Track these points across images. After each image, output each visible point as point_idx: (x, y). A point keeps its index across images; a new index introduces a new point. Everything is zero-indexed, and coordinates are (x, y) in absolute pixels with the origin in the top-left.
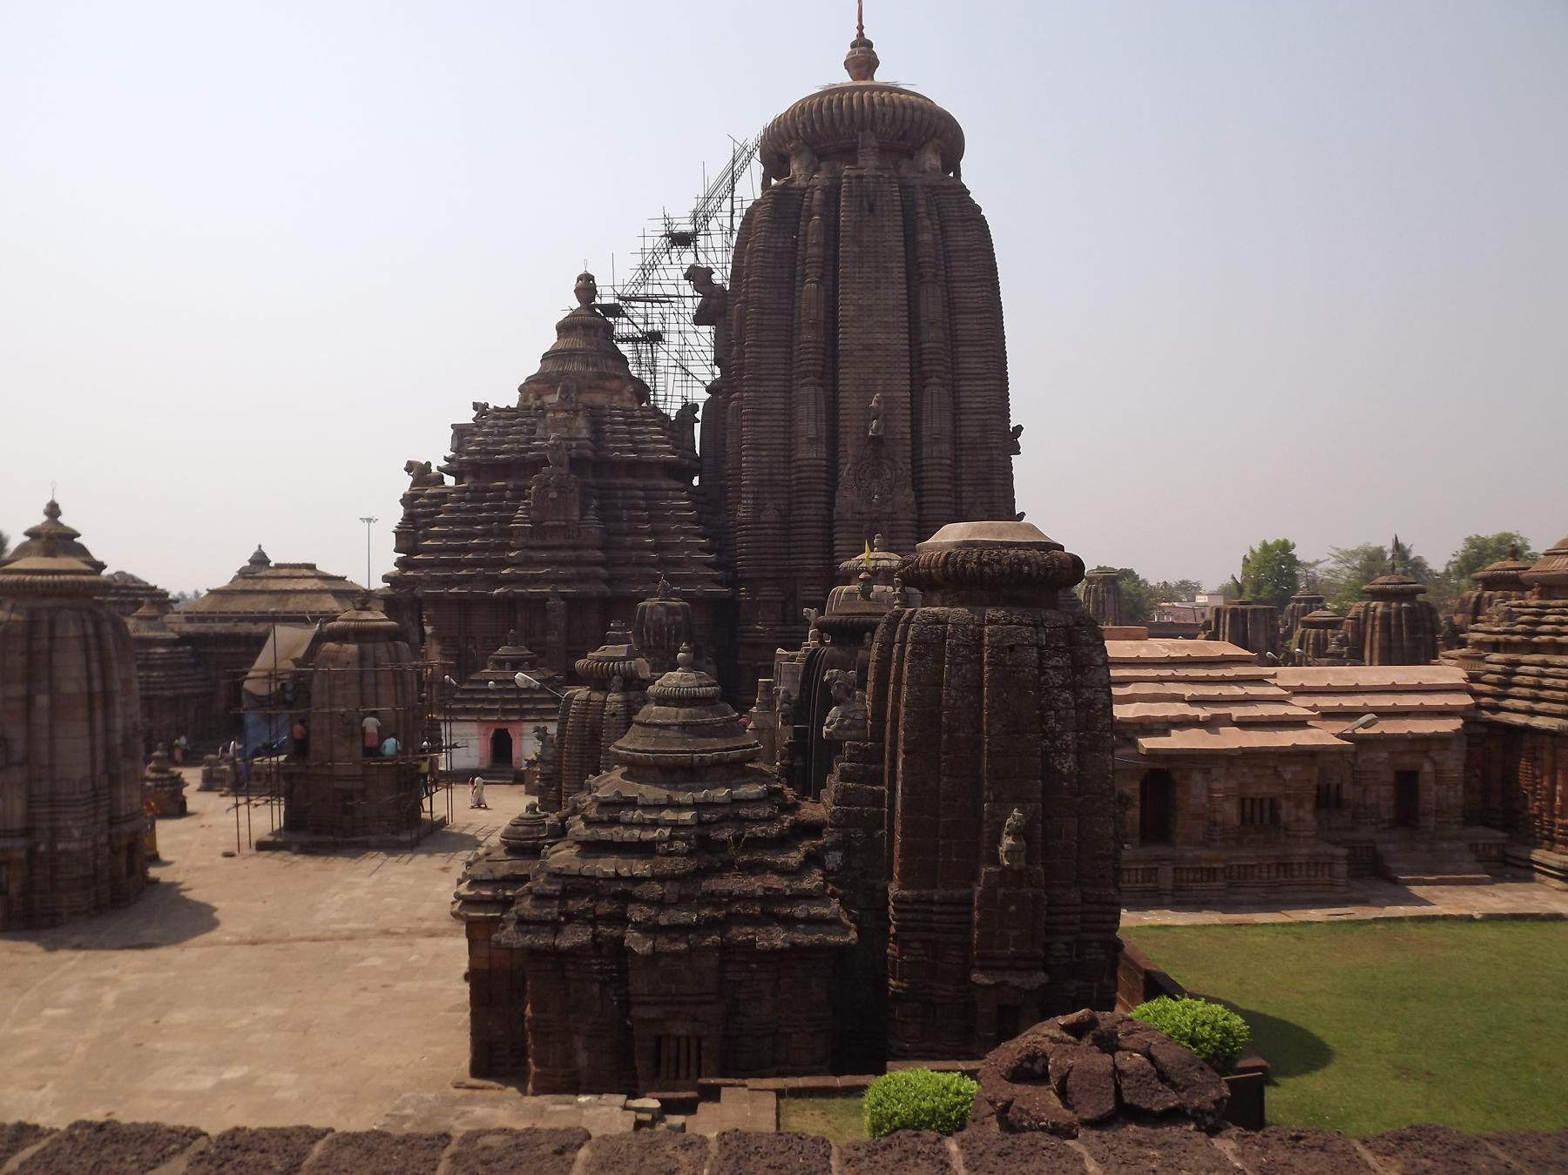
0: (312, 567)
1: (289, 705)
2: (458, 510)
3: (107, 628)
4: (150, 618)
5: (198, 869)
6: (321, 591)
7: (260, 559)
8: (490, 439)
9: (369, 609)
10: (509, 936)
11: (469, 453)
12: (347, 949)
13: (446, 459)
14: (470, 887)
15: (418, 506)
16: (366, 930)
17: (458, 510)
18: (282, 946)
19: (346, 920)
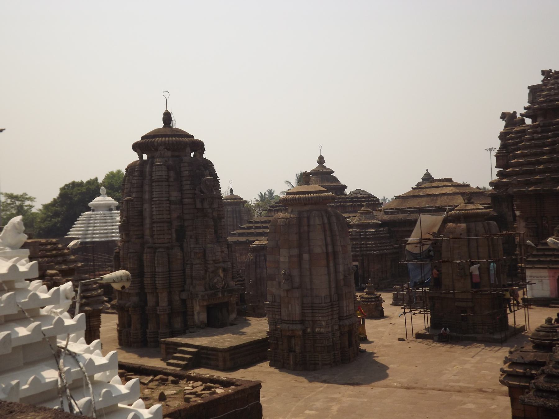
0: (450, 180)
1: (430, 258)
2: (533, 139)
3: (334, 219)
4: (366, 213)
5: (386, 346)
6: (455, 194)
7: (428, 178)
8: (552, 92)
9: (472, 203)
10: (530, 397)
11: (539, 103)
12: (456, 397)
13: (525, 108)
14: (510, 366)
15: (509, 139)
16: (470, 388)
17: (533, 139)
18: (422, 391)
19: (458, 381)
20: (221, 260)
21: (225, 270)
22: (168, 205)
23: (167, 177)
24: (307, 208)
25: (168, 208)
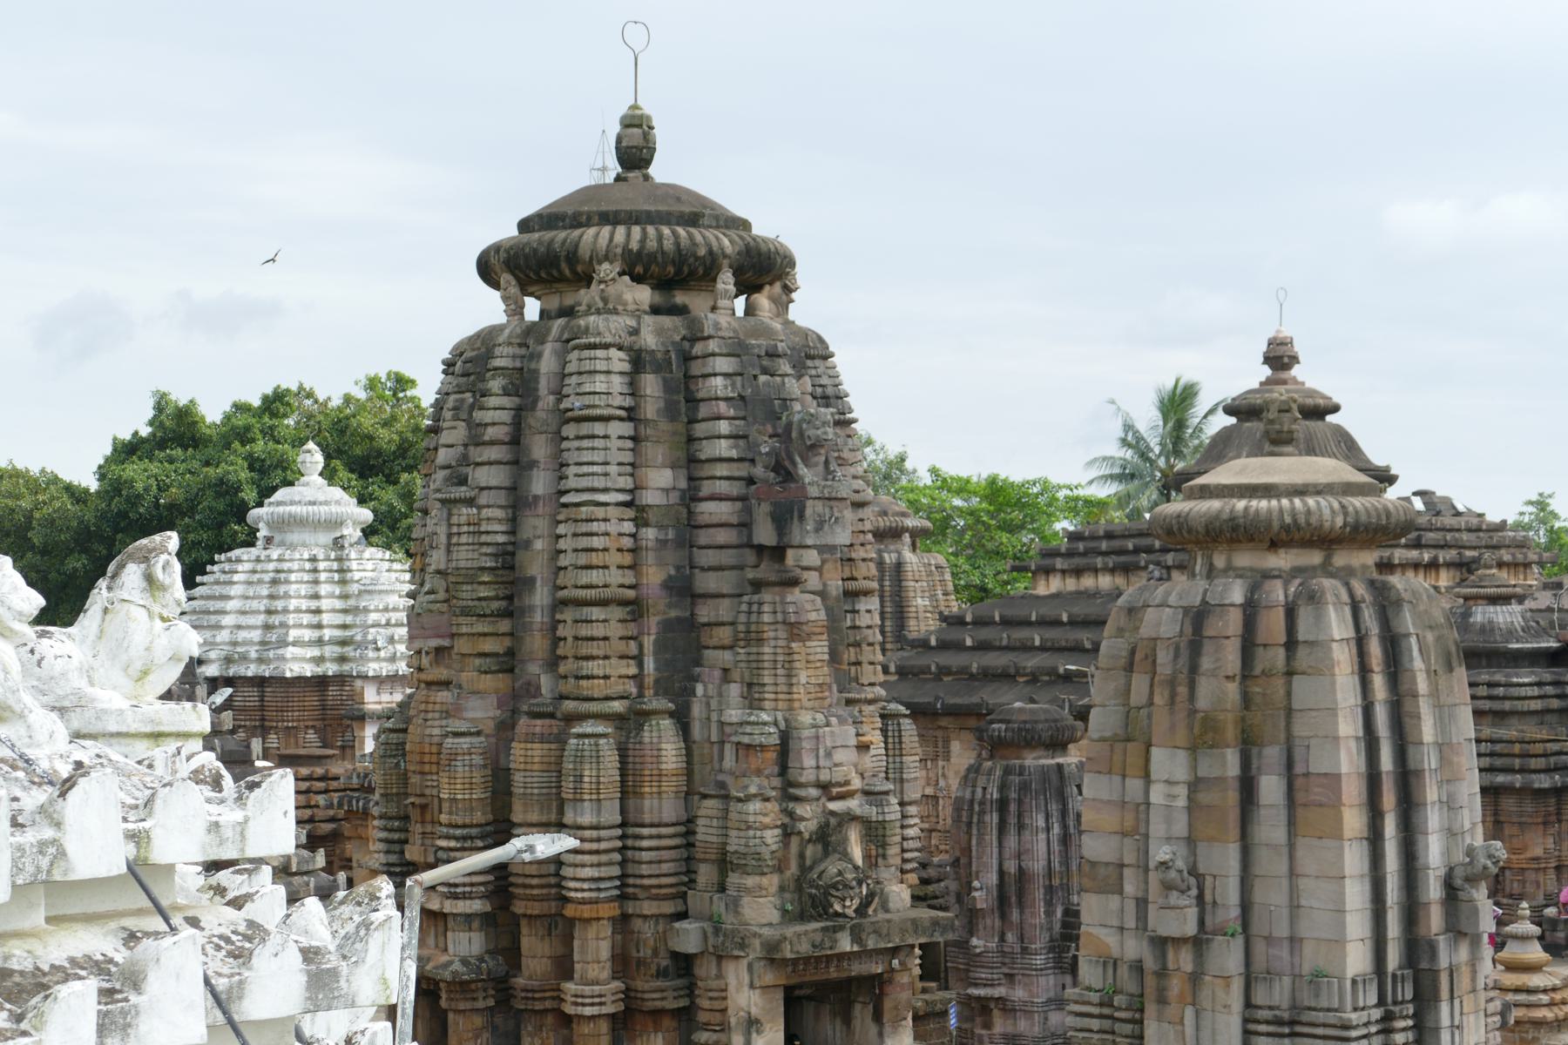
20: (857, 783)
21: (875, 834)
22: (628, 527)
23: (628, 402)
24: (1281, 560)
25: (627, 542)
